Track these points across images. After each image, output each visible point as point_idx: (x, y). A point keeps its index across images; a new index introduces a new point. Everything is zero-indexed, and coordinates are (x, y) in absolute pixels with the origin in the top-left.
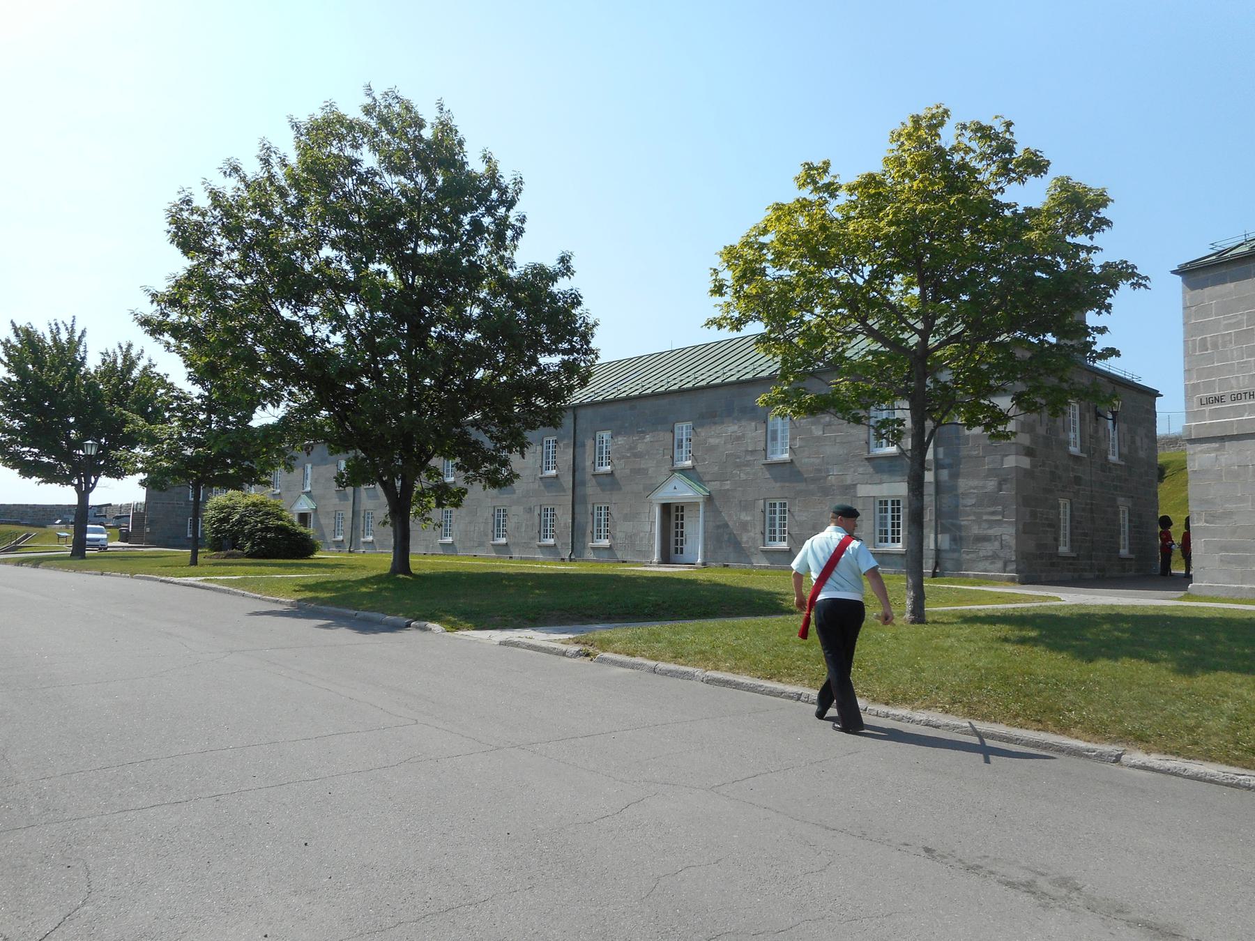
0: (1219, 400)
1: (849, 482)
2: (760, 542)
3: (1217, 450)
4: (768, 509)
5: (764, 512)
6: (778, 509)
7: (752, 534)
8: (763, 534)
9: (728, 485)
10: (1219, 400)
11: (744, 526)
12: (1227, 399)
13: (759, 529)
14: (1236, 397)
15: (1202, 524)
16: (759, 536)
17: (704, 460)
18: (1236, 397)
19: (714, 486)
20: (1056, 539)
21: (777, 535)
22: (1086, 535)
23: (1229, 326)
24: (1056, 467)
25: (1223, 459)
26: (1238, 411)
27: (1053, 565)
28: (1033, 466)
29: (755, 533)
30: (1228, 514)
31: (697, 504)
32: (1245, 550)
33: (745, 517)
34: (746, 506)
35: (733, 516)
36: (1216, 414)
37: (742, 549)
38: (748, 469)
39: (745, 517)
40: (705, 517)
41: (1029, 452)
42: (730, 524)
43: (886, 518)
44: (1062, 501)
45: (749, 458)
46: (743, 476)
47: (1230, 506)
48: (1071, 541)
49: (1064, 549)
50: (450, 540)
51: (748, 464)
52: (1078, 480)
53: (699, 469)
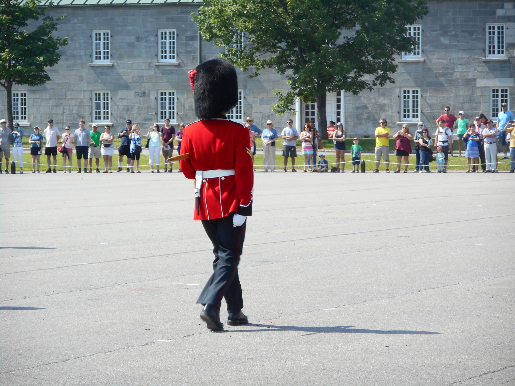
1: (470, 77)
2: (396, 119)
4: (402, 95)
11: (382, 107)
13: (395, 109)
16: (396, 115)
42: (370, 106)
43: (497, 101)
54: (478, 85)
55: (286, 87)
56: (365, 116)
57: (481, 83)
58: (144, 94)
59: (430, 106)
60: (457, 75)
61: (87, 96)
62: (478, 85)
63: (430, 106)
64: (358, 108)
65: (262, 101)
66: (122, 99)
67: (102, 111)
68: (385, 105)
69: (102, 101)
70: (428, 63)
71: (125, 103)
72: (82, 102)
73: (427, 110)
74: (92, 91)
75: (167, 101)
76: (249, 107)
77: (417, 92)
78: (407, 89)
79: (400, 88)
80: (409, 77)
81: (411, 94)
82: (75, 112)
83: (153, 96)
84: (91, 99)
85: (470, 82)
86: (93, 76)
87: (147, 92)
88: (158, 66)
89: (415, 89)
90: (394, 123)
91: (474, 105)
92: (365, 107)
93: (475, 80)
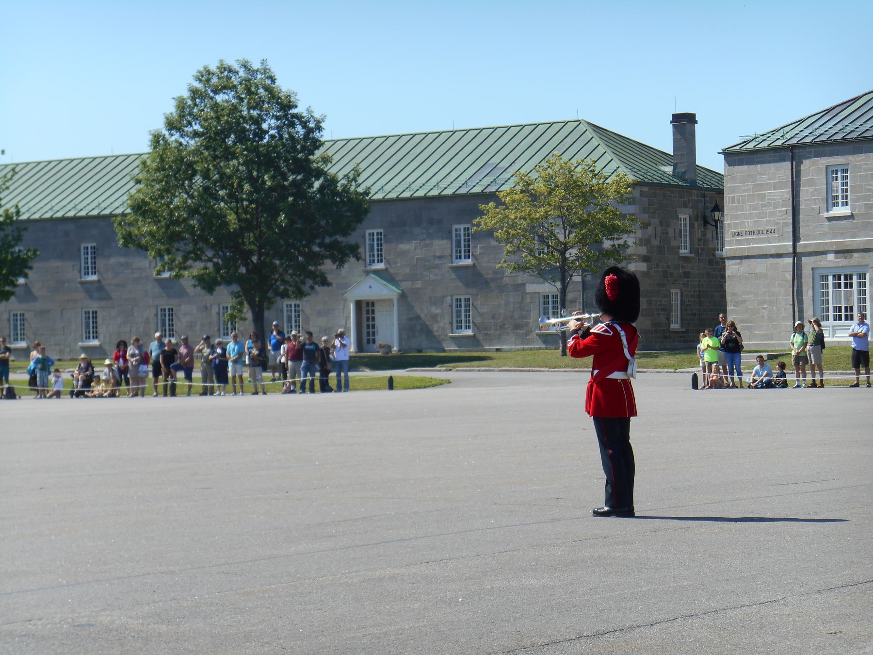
0: (740, 234)
1: (520, 282)
2: (449, 330)
3: (739, 264)
5: (451, 306)
6: (463, 303)
7: (442, 324)
8: (451, 323)
9: (419, 284)
10: (740, 234)
11: (435, 318)
12: (743, 234)
13: (447, 320)
14: (748, 233)
15: (732, 307)
16: (448, 326)
17: (396, 263)
18: (748, 233)
19: (406, 285)
20: (668, 319)
21: (463, 325)
22: (694, 314)
23: (745, 191)
24: (668, 267)
25: (741, 269)
26: (748, 242)
27: (665, 337)
28: (649, 268)
29: (444, 322)
30: (744, 302)
31: (391, 300)
32: (751, 322)
33: (435, 310)
34: (436, 301)
35: (424, 310)
36: (739, 242)
37: (435, 336)
38: (436, 271)
39: (435, 310)
40: (399, 311)
41: (646, 259)
42: (422, 316)
43: (548, 308)
44: (673, 291)
45: (437, 262)
46: (432, 277)
47: (745, 297)
48: (682, 320)
49: (675, 326)
50: (95, 343)
51: (436, 267)
52: (687, 275)
53: (392, 271)
54: (528, 291)
55: (230, 302)
56: (418, 328)
57: (531, 288)
58: (206, 308)
59: (481, 315)
60: (506, 280)
61: (153, 311)
62: (528, 291)
63: (481, 315)
64: (411, 319)
65: (319, 314)
66: (185, 314)
67: (463, 318)
68: (437, 315)
69: (463, 308)
70: (478, 266)
71: (188, 318)
72: (148, 319)
73: (478, 320)
74: (157, 306)
75: (463, 308)
76: (307, 320)
77: (469, 299)
78: (459, 297)
79: (452, 296)
80: (460, 284)
81: (463, 303)
82: (141, 329)
83: (215, 310)
84: (156, 315)
85: (520, 287)
86: (157, 290)
87: (208, 306)
88: (83, 283)
89: (467, 297)
90: (446, 336)
91: (524, 313)
92: (418, 318)
93: (524, 284)
